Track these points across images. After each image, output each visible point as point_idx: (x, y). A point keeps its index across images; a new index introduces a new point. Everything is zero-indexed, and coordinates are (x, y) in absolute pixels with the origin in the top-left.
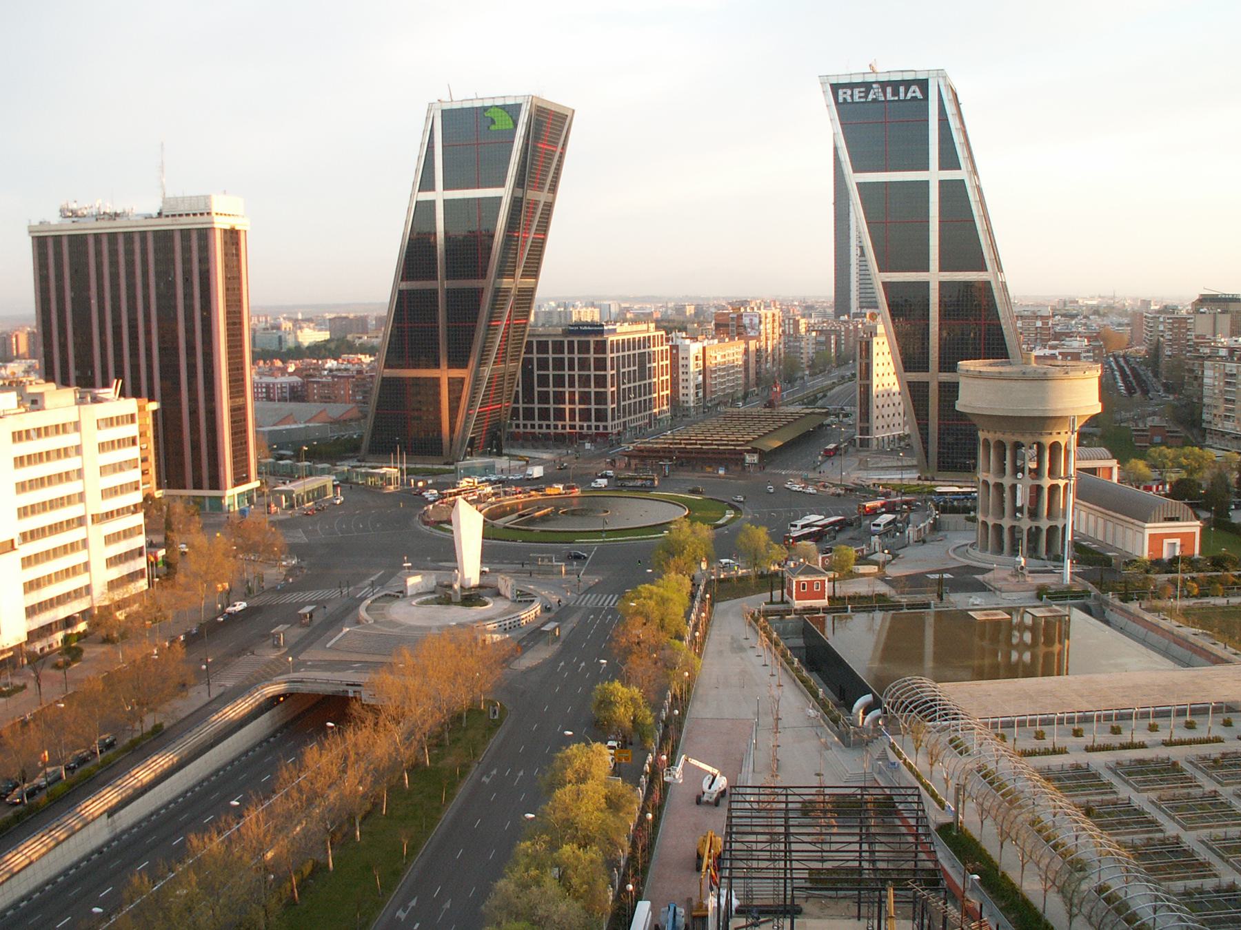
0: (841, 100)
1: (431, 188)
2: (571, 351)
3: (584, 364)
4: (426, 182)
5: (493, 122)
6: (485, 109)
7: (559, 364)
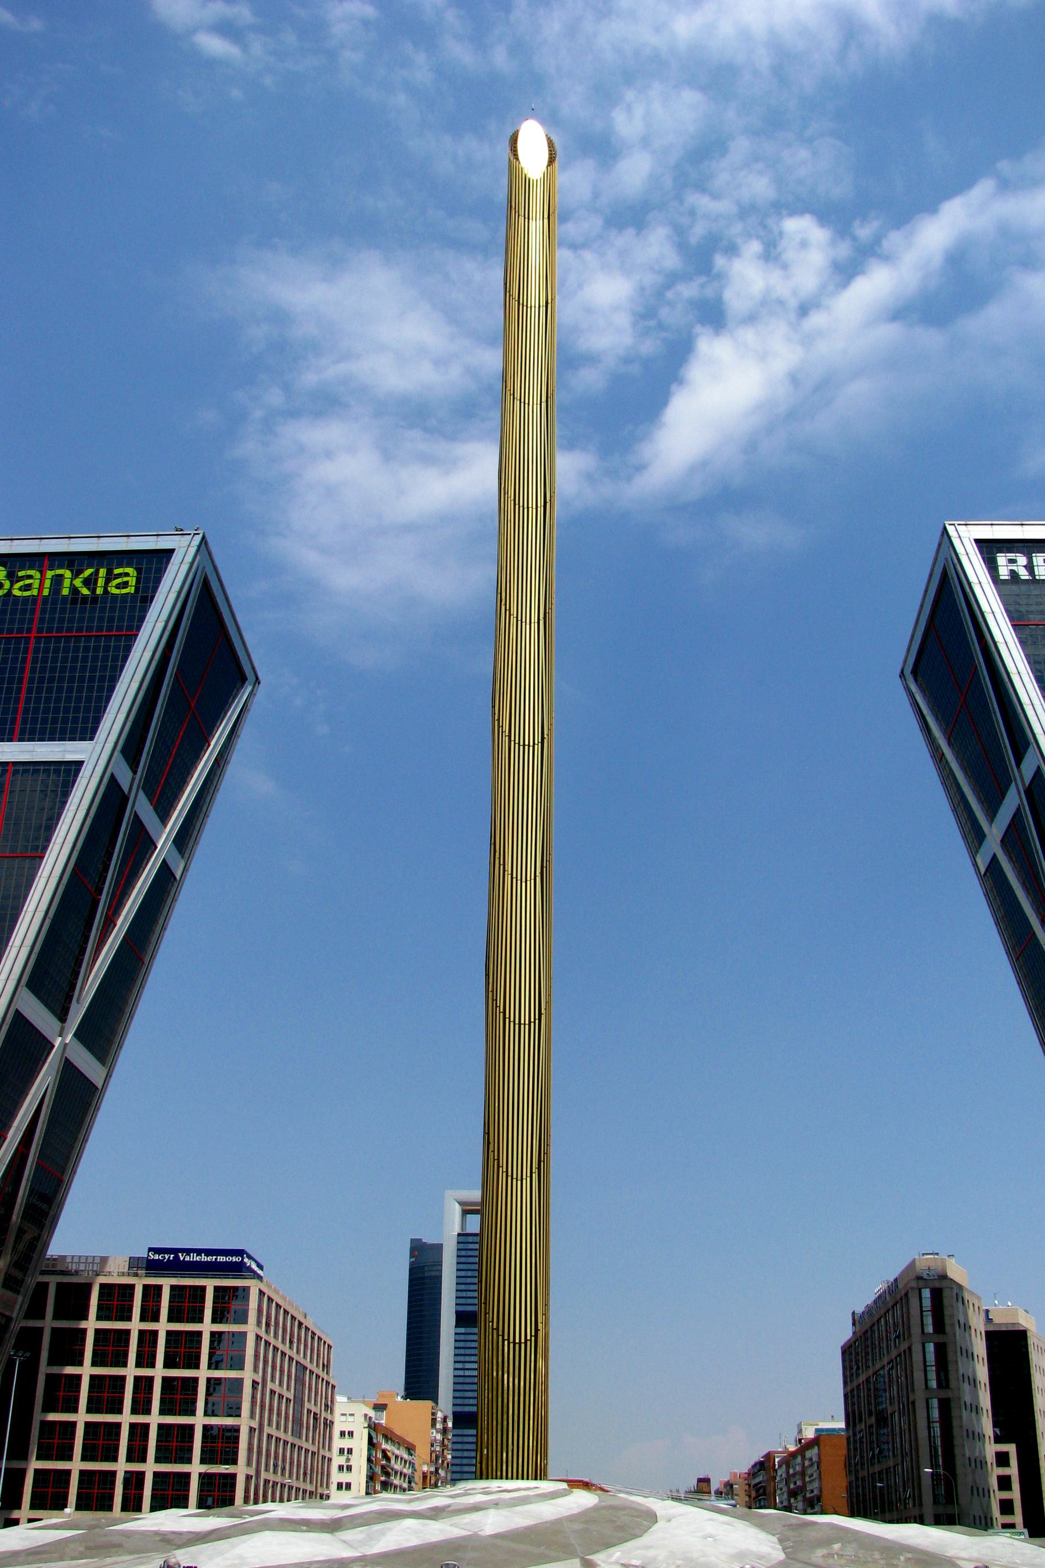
0: (1004, 573)
2: (150, 1313)
3: (184, 1349)
7: (111, 1348)
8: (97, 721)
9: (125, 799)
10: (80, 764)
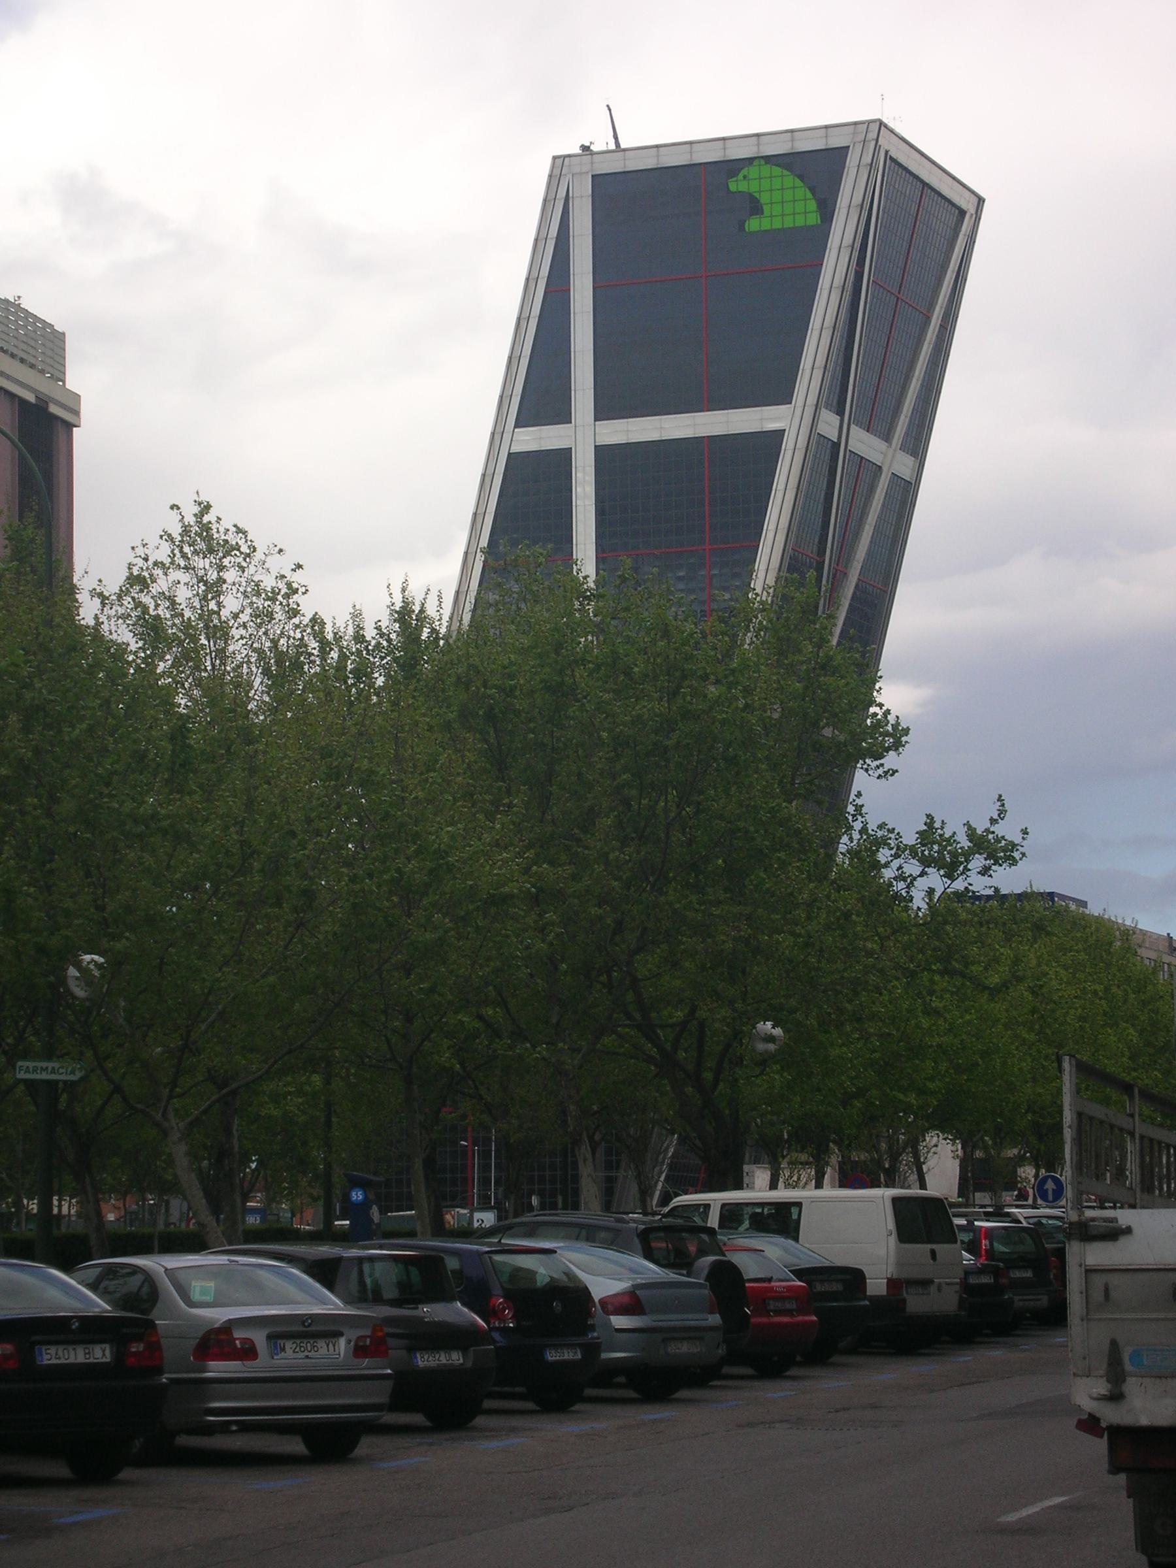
1: (562, 415)
5: (756, 208)
6: (732, 167)
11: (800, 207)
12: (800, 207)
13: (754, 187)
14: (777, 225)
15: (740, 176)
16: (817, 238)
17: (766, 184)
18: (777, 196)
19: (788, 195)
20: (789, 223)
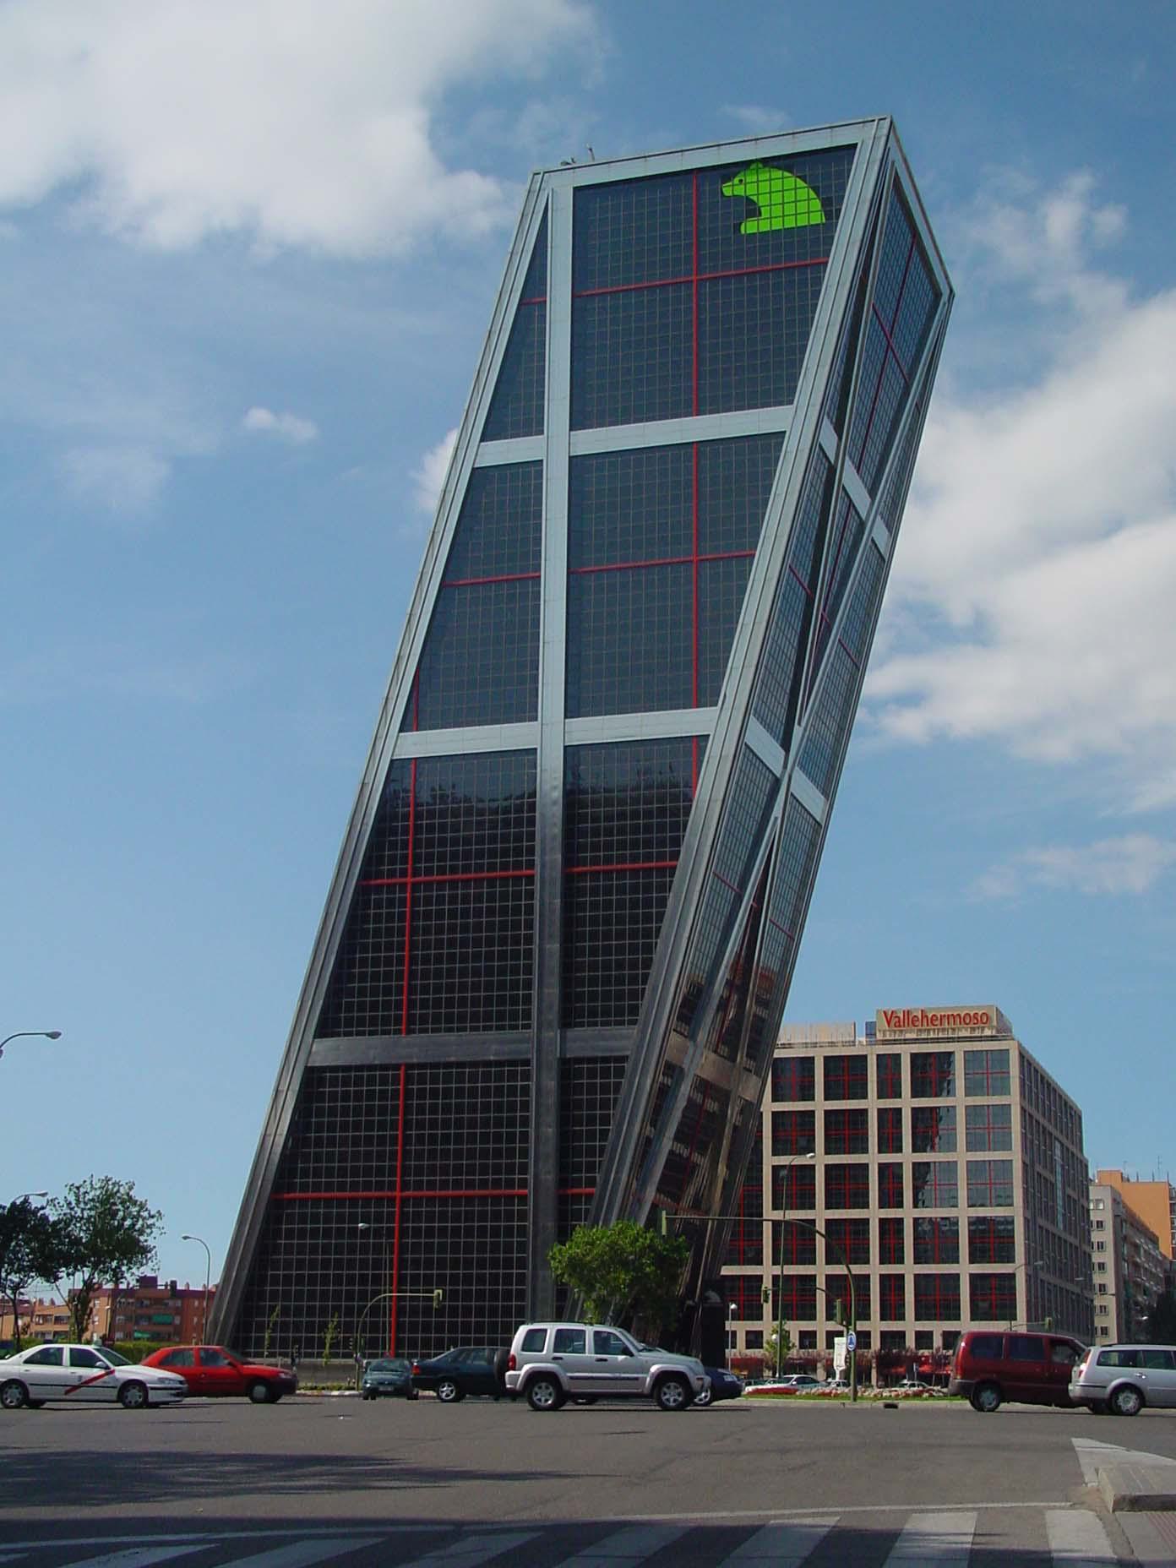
1: (533, 425)
2: (889, 1087)
4: (512, 408)
5: (752, 209)
7: (846, 1132)
8: (794, 379)
9: (832, 470)
10: (781, 434)
11: (802, 207)
12: (802, 207)
13: (751, 191)
14: (777, 225)
15: (736, 180)
16: (817, 241)
17: (764, 187)
18: (777, 198)
19: (790, 196)
20: (790, 223)
